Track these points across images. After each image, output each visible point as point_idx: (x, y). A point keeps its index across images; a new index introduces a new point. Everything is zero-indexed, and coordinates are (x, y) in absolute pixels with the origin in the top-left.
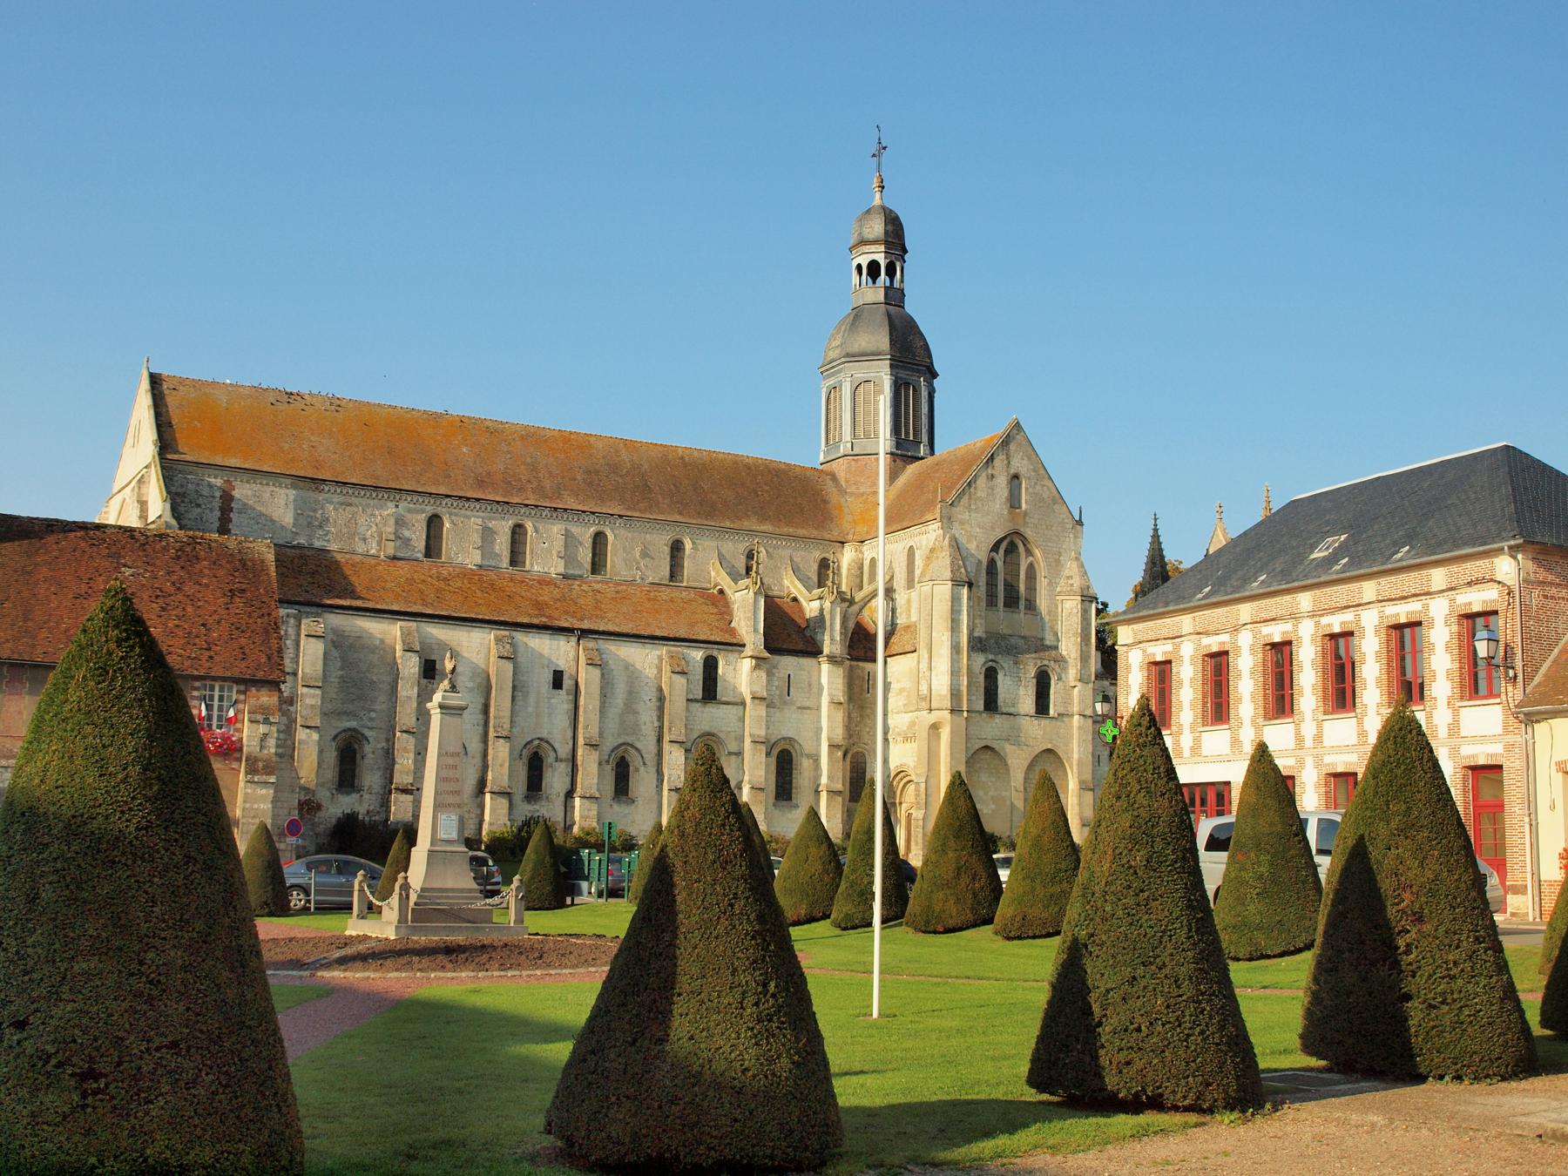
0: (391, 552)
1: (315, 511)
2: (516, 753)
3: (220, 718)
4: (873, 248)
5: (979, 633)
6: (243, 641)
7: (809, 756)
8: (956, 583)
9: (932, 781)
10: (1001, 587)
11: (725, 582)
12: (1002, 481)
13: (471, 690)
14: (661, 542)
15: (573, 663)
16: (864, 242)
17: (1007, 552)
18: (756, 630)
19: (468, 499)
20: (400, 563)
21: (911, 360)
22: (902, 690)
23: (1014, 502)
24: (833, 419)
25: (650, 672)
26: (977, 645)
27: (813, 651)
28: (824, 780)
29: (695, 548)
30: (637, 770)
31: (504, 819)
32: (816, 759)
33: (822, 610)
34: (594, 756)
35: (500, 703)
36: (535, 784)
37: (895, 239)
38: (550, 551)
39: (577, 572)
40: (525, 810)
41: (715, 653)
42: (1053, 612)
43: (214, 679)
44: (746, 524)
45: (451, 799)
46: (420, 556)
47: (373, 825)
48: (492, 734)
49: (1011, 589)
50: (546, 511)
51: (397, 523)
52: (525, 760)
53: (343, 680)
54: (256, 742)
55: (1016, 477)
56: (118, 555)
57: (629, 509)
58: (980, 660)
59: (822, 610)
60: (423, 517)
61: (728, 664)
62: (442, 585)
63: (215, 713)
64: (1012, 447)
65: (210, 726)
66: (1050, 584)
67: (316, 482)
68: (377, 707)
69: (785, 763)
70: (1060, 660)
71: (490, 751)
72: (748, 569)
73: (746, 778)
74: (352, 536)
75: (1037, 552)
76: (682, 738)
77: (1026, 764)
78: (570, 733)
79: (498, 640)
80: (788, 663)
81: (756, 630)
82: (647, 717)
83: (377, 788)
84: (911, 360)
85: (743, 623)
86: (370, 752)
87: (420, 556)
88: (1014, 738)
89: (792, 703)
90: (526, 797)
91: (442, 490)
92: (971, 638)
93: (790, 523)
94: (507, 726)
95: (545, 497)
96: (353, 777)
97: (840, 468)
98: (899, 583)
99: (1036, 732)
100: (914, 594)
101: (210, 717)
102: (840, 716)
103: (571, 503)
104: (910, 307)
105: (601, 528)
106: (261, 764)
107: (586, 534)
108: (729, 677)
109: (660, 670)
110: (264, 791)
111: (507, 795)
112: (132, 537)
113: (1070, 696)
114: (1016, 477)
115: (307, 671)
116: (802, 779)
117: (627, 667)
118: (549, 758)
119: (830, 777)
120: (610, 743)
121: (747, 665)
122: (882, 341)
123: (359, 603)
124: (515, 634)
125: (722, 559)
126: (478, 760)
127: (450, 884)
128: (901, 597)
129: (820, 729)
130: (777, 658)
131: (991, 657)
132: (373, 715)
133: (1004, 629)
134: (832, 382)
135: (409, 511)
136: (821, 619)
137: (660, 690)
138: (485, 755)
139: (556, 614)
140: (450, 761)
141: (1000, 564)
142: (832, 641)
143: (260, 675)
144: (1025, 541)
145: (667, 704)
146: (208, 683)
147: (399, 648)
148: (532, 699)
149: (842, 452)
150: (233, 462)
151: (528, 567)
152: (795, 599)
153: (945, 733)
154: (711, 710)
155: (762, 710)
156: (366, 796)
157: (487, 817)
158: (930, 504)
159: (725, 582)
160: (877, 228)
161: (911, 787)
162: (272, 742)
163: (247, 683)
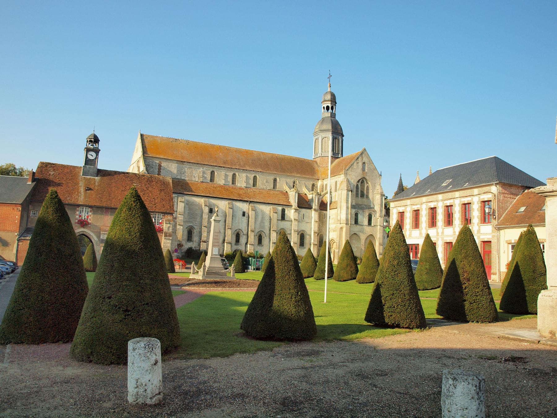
0: (201, 180)
5: (354, 204)
8: (348, 190)
10: (360, 192)
11: (287, 189)
12: (360, 164)
14: (271, 179)
21: (337, 132)
23: (363, 169)
25: (268, 212)
26: (353, 207)
27: (310, 208)
28: (312, 241)
29: (280, 180)
32: (310, 236)
34: (253, 234)
36: (238, 241)
37: (333, 100)
40: (235, 247)
44: (293, 174)
45: (217, 244)
47: (196, 251)
48: (227, 228)
49: (362, 192)
54: (167, 229)
55: (364, 163)
56: (132, 180)
58: (354, 211)
60: (210, 171)
61: (288, 210)
64: (363, 155)
70: (375, 211)
72: (294, 186)
74: (191, 176)
75: (369, 183)
79: (229, 204)
80: (304, 211)
82: (267, 224)
83: (197, 241)
84: (337, 132)
86: (195, 232)
88: (362, 231)
93: (305, 174)
97: (318, 160)
98: (333, 190)
99: (368, 230)
100: (337, 193)
101: (155, 222)
102: (317, 225)
103: (248, 168)
107: (251, 176)
113: (377, 221)
116: (306, 241)
117: (262, 211)
118: (241, 234)
119: (314, 241)
120: (257, 231)
121: (293, 211)
122: (329, 127)
125: (287, 183)
126: (223, 235)
127: (216, 266)
128: (333, 194)
129: (312, 228)
130: (301, 209)
133: (360, 203)
134: (316, 137)
136: (312, 199)
138: (225, 233)
140: (216, 234)
141: (359, 186)
142: (315, 205)
143: (168, 212)
144: (366, 180)
147: (203, 205)
148: (237, 219)
150: (162, 157)
153: (344, 230)
154: (283, 222)
155: (296, 223)
158: (342, 169)
159: (287, 189)
160: (329, 97)
161: (335, 244)
162: (171, 229)
163: (165, 213)
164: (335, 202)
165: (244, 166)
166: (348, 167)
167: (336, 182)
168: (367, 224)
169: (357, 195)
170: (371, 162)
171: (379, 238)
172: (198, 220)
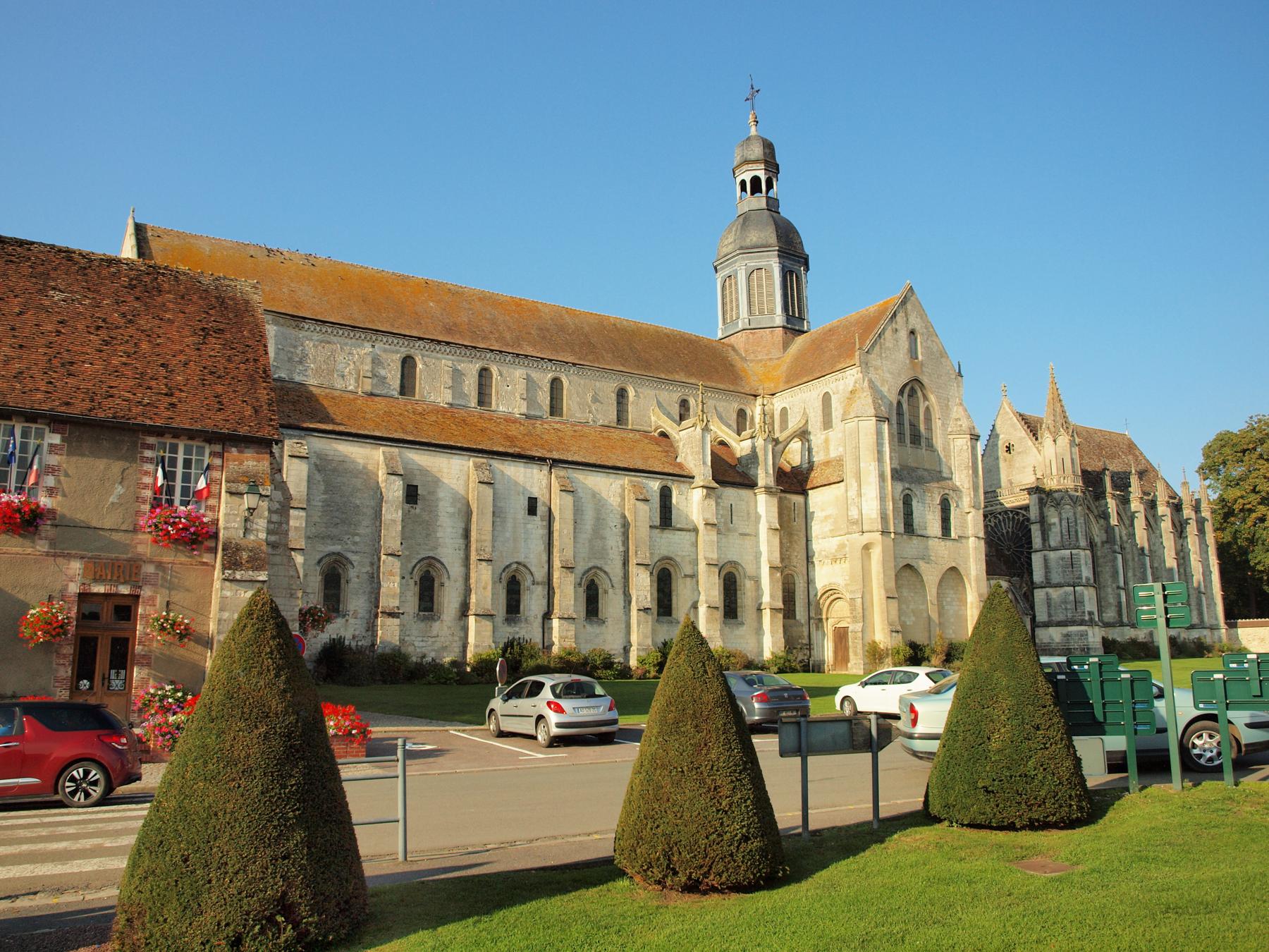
0: (368, 388)
1: (295, 347)
3: (185, 491)
4: (754, 166)
6: (220, 389)
7: (751, 578)
8: (880, 419)
9: (867, 597)
12: (903, 334)
14: (608, 388)
15: (545, 491)
17: (910, 396)
18: (704, 463)
19: (439, 342)
20: (376, 399)
22: (827, 518)
24: (733, 301)
25: (614, 501)
26: (897, 475)
27: (751, 484)
28: (766, 599)
30: (606, 592)
31: (488, 641)
32: (757, 581)
33: (754, 448)
35: (481, 528)
36: (513, 607)
38: (514, 392)
40: (507, 632)
41: (669, 484)
42: (946, 448)
43: (177, 433)
47: (360, 651)
48: (474, 557)
49: (914, 427)
50: (509, 357)
51: (373, 362)
52: (504, 583)
53: (327, 504)
54: (237, 524)
56: (46, 276)
57: (580, 359)
59: (754, 448)
60: (397, 357)
61: (681, 493)
62: (418, 418)
64: (909, 306)
66: (943, 424)
67: (297, 319)
68: (361, 531)
70: (956, 490)
71: (473, 575)
73: (702, 598)
75: (932, 397)
76: (647, 562)
77: (937, 580)
78: (545, 558)
79: (477, 467)
80: (731, 494)
81: (704, 463)
82: (613, 542)
85: (690, 458)
86: (355, 577)
87: (396, 394)
89: (735, 530)
90: (507, 620)
92: (892, 470)
93: (710, 379)
94: (489, 549)
95: (508, 345)
96: (338, 601)
97: (739, 341)
99: (942, 552)
100: (835, 434)
101: (170, 490)
102: (776, 541)
104: (785, 212)
105: (557, 374)
106: (245, 555)
109: (623, 499)
111: (489, 616)
112: (70, 259)
113: (965, 521)
114: (912, 332)
116: (746, 599)
117: (594, 495)
118: (526, 582)
119: (772, 596)
120: (581, 568)
121: (697, 495)
122: (770, 236)
124: (492, 462)
125: (660, 405)
126: (460, 584)
128: (817, 438)
129: (762, 553)
130: (721, 489)
131: (907, 485)
132: (357, 539)
134: (727, 272)
135: (385, 351)
136: (753, 457)
137: (624, 517)
138: (467, 578)
139: (527, 446)
141: (905, 406)
142: (764, 476)
143: (243, 430)
146: (169, 441)
147: (382, 475)
148: (509, 525)
149: (740, 326)
151: (493, 408)
152: (722, 443)
153: (876, 554)
154: (668, 535)
155: (713, 536)
156: (352, 621)
157: (472, 639)
159: (669, 427)
160: (757, 151)
161: (839, 604)
162: (261, 524)
163: (225, 440)
164: (827, 463)
165: (517, 341)
166: (868, 343)
167: (826, 398)
168: (939, 534)
170: (931, 333)
171: (977, 580)
172: (361, 531)
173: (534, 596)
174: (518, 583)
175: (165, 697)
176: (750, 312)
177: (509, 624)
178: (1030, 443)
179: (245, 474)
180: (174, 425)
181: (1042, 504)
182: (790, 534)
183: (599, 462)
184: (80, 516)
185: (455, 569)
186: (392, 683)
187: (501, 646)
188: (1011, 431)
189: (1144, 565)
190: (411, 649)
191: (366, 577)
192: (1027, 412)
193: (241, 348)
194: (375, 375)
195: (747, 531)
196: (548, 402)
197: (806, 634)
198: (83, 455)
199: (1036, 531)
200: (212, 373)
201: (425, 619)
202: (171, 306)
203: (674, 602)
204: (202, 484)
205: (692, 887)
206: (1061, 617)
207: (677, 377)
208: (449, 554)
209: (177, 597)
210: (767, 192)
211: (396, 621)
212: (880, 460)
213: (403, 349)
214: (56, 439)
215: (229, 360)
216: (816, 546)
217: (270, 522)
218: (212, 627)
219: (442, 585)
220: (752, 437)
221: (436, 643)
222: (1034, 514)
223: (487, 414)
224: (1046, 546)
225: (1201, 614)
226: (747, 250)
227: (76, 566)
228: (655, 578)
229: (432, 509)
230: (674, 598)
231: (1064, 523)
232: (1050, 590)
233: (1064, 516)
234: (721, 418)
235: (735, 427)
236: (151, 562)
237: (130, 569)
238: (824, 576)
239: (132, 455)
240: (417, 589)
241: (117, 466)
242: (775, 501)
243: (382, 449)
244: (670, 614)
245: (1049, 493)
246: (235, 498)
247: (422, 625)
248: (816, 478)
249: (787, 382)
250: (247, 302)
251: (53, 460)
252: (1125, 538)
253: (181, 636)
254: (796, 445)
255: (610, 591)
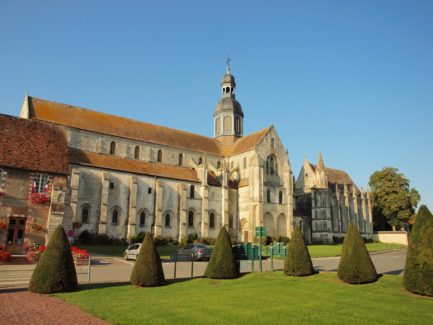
0: (100, 152)
1: (77, 138)
2: (137, 212)
3: (42, 188)
4: (228, 84)
5: (265, 181)
6: (53, 159)
7: (219, 215)
8: (260, 166)
9: (254, 222)
10: (269, 169)
12: (269, 140)
13: (124, 193)
14: (176, 154)
15: (154, 186)
16: (225, 82)
18: (205, 178)
19: (123, 138)
20: (102, 155)
21: (238, 113)
22: (243, 197)
23: (272, 146)
24: (218, 127)
26: (265, 184)
27: (220, 185)
28: (223, 221)
29: (186, 156)
30: (172, 218)
31: (134, 233)
32: (221, 216)
33: (222, 174)
34: (161, 214)
35: (133, 197)
38: (146, 154)
39: (154, 161)
40: (140, 230)
41: (194, 185)
43: (40, 172)
44: (199, 151)
46: (109, 153)
47: (93, 234)
48: (130, 206)
49: (272, 169)
50: (145, 143)
51: (102, 143)
52: (140, 214)
56: (4, 124)
58: (266, 188)
59: (222, 174)
62: (115, 162)
63: (40, 186)
64: (272, 131)
65: (37, 192)
66: (281, 168)
67: (78, 130)
68: (95, 197)
69: (212, 217)
70: (284, 189)
71: (130, 212)
73: (203, 221)
74: (88, 146)
75: (278, 160)
78: (153, 207)
79: (133, 178)
80: (213, 188)
81: (205, 178)
82: (175, 202)
83: (94, 222)
84: (238, 113)
85: (201, 177)
87: (109, 153)
88: (275, 210)
89: (214, 200)
90: (140, 226)
91: (116, 135)
92: (264, 182)
93: (210, 151)
94: (135, 204)
95: (145, 139)
96: (87, 219)
98: (241, 167)
99: (279, 208)
100: (247, 170)
101: (37, 188)
102: (227, 203)
103: (152, 141)
104: (237, 99)
105: (160, 149)
106: (58, 207)
107: (156, 150)
108: (198, 191)
109: (179, 189)
110: (59, 218)
111: (134, 225)
112: (11, 119)
113: (287, 199)
114: (273, 139)
115: (74, 184)
117: (170, 187)
118: (147, 214)
119: (225, 221)
120: (164, 210)
121: (203, 188)
122: (231, 106)
123: (91, 165)
124: (138, 176)
125: (193, 159)
126: (126, 214)
128: (242, 171)
129: (223, 207)
130: (210, 187)
132: (94, 199)
134: (217, 117)
135: (106, 140)
136: (221, 176)
137: (179, 194)
138: (128, 212)
141: (269, 162)
142: (224, 183)
143: (59, 172)
145: (181, 199)
146: (38, 174)
147: (103, 179)
149: (221, 135)
151: (140, 159)
152: (212, 172)
153: (258, 208)
154: (193, 201)
155: (207, 201)
156: (91, 225)
159: (195, 166)
160: (229, 79)
161: (246, 224)
162: (63, 198)
163: (54, 174)
164: (244, 179)
165: (148, 138)
166: (258, 143)
167: (245, 159)
168: (278, 203)
169: (267, 173)
171: (290, 217)
173: (149, 219)
174: (144, 215)
175: (33, 246)
176: (224, 130)
177: (141, 227)
178: (313, 174)
179: (59, 184)
180: (39, 170)
181: (315, 193)
182: (232, 201)
183: (172, 177)
184: (11, 195)
185: (124, 210)
186: (103, 245)
187: (138, 234)
188: (308, 170)
189: (347, 214)
190: (109, 234)
191: (96, 211)
192: (313, 164)
193: (59, 147)
194: (102, 148)
195: (218, 200)
196: (157, 157)
197: (236, 233)
198: (13, 178)
199: (313, 202)
200: (51, 154)
201: (113, 225)
202: (40, 134)
203: (194, 222)
204: (47, 186)
205: (143, 286)
206: (320, 229)
207: (199, 151)
208: (123, 204)
209: (38, 218)
210: (231, 92)
211: (105, 225)
212: (260, 179)
213: (111, 140)
214: (5, 173)
215: (56, 151)
216: (240, 205)
217: (65, 198)
218: (48, 227)
219: (120, 214)
220: (221, 171)
221: (117, 232)
222: (313, 196)
223: (137, 161)
224: (316, 207)
225: (365, 229)
226: (224, 110)
227: (9, 209)
228: (188, 214)
229: (118, 191)
230: (194, 220)
231: (322, 200)
232: (317, 221)
233: (322, 197)
234: (212, 164)
235: (217, 166)
236: (31, 208)
237: (25, 210)
238: (242, 215)
239: (27, 179)
240: (112, 216)
241: (22, 182)
242: (227, 191)
243: (103, 171)
244: (192, 226)
245: (318, 190)
246: (56, 191)
247: (113, 227)
248: (241, 184)
249: (234, 153)
250: (62, 133)
251: (4, 179)
252: (342, 205)
253: (38, 230)
254: (235, 173)
255: (173, 218)
